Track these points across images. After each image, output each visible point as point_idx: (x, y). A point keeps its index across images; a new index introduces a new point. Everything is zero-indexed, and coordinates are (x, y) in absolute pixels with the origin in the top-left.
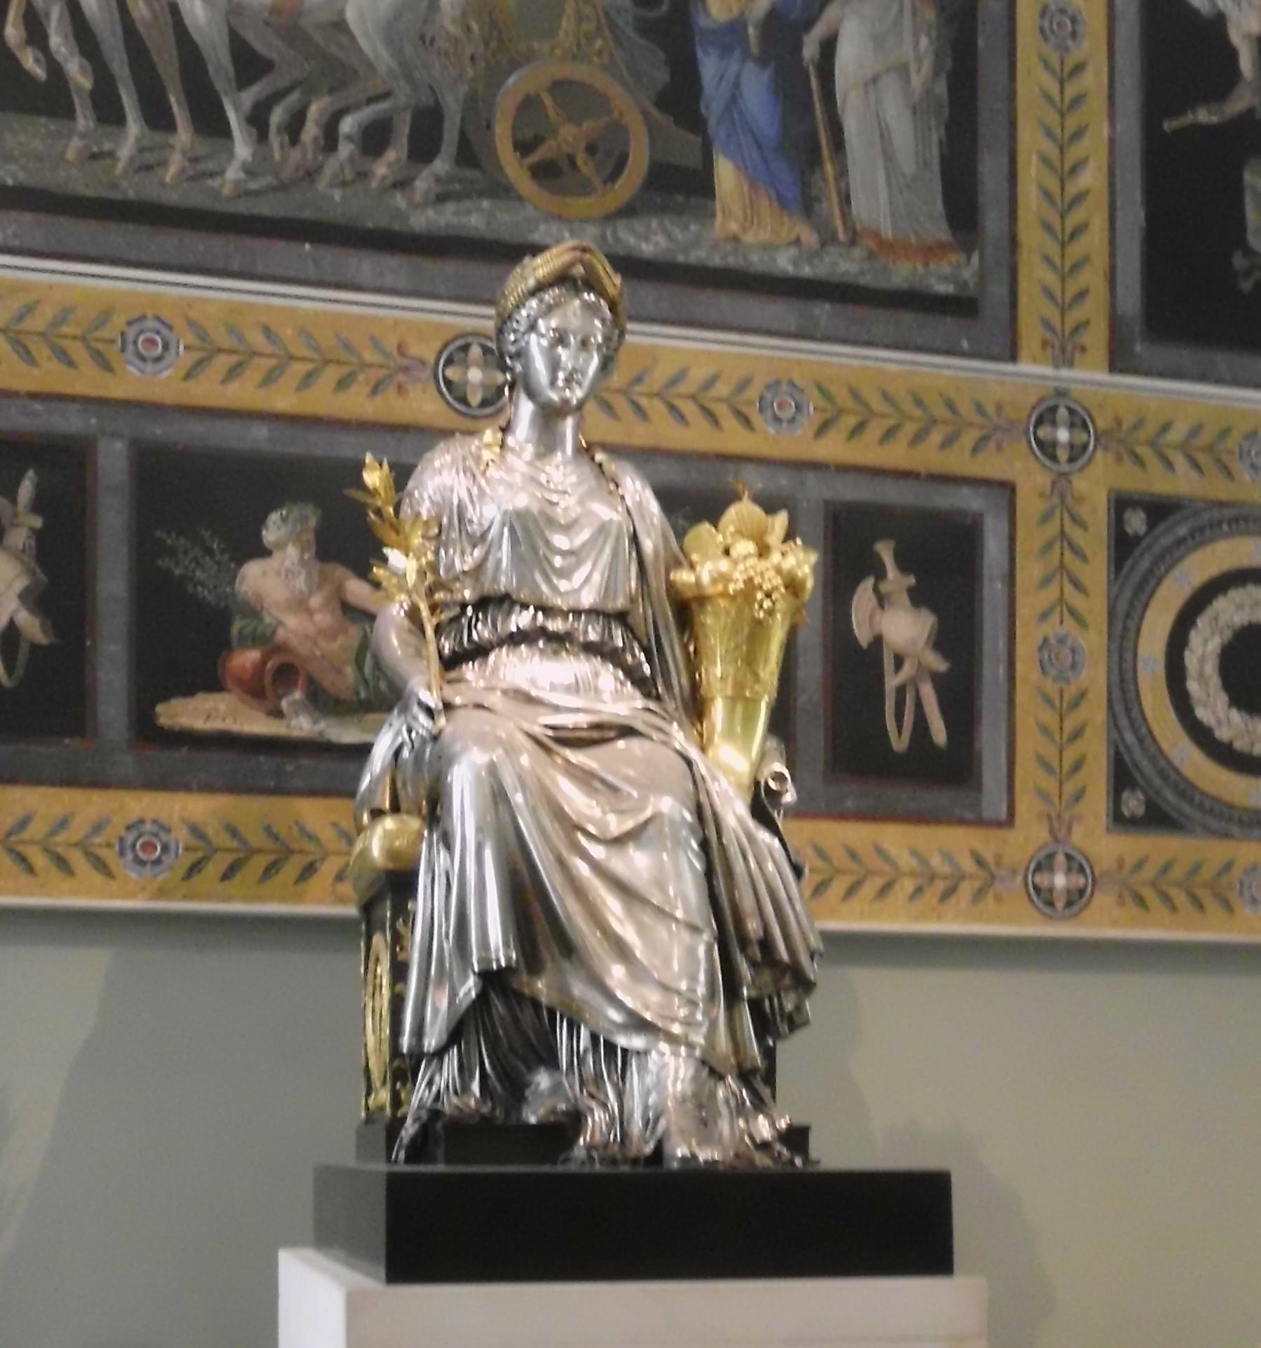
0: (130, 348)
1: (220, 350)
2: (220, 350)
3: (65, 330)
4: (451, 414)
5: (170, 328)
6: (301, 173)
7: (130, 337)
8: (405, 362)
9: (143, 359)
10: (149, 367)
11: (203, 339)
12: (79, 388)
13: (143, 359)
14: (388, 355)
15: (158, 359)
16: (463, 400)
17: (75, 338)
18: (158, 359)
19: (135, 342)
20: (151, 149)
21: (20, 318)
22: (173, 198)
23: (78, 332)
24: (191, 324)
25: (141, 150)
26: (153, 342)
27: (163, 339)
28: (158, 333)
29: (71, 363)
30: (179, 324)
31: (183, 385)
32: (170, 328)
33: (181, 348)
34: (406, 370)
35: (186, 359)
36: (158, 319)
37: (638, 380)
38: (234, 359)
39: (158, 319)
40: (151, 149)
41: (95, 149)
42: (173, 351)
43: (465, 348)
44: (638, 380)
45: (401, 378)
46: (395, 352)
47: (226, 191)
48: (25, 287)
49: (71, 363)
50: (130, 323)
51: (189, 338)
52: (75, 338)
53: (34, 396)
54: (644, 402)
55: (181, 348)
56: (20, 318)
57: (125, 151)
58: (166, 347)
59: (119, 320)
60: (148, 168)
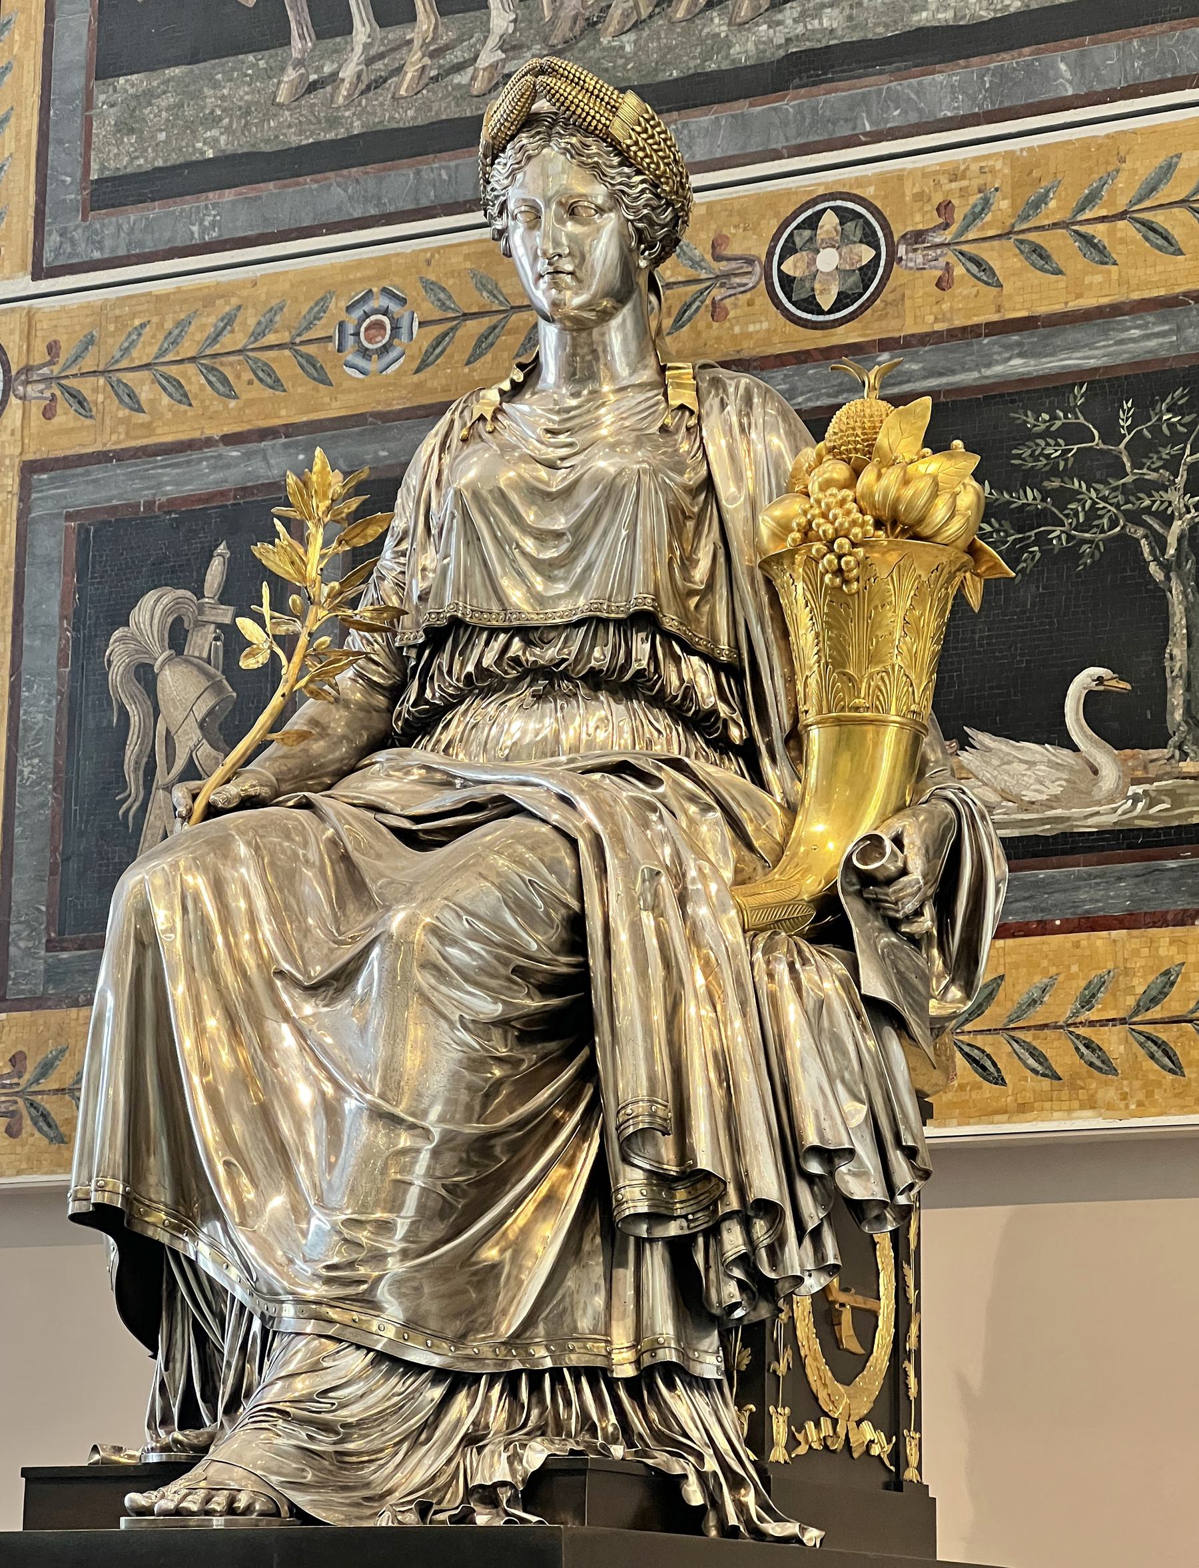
0: (350, 340)
1: (466, 316)
2: (466, 316)
3: (271, 339)
4: (791, 327)
5: (403, 301)
6: (581, 23)
7: (351, 329)
8: (724, 266)
9: (365, 353)
10: (372, 366)
11: (443, 306)
12: (285, 415)
13: (365, 353)
14: (696, 264)
15: (385, 349)
16: (810, 304)
17: (280, 346)
18: (385, 349)
19: (357, 334)
20: (381, 56)
21: (215, 338)
22: (408, 117)
23: (285, 337)
24: (430, 286)
25: (369, 62)
26: (379, 325)
27: (391, 319)
28: (385, 312)
29: (277, 384)
30: (414, 292)
31: (416, 378)
32: (403, 301)
33: (416, 324)
34: (722, 278)
35: (423, 339)
36: (385, 291)
37: (1090, 200)
38: (487, 322)
39: (385, 291)
40: (381, 56)
41: (313, 77)
42: (404, 331)
43: (812, 223)
44: (1090, 200)
45: (717, 293)
46: (708, 257)
47: (478, 86)
48: (223, 292)
49: (277, 384)
50: (349, 309)
51: (429, 309)
52: (280, 346)
53: (230, 440)
54: (1099, 231)
55: (416, 324)
56: (215, 338)
57: (348, 72)
58: (395, 328)
59: (337, 307)
60: (379, 83)
